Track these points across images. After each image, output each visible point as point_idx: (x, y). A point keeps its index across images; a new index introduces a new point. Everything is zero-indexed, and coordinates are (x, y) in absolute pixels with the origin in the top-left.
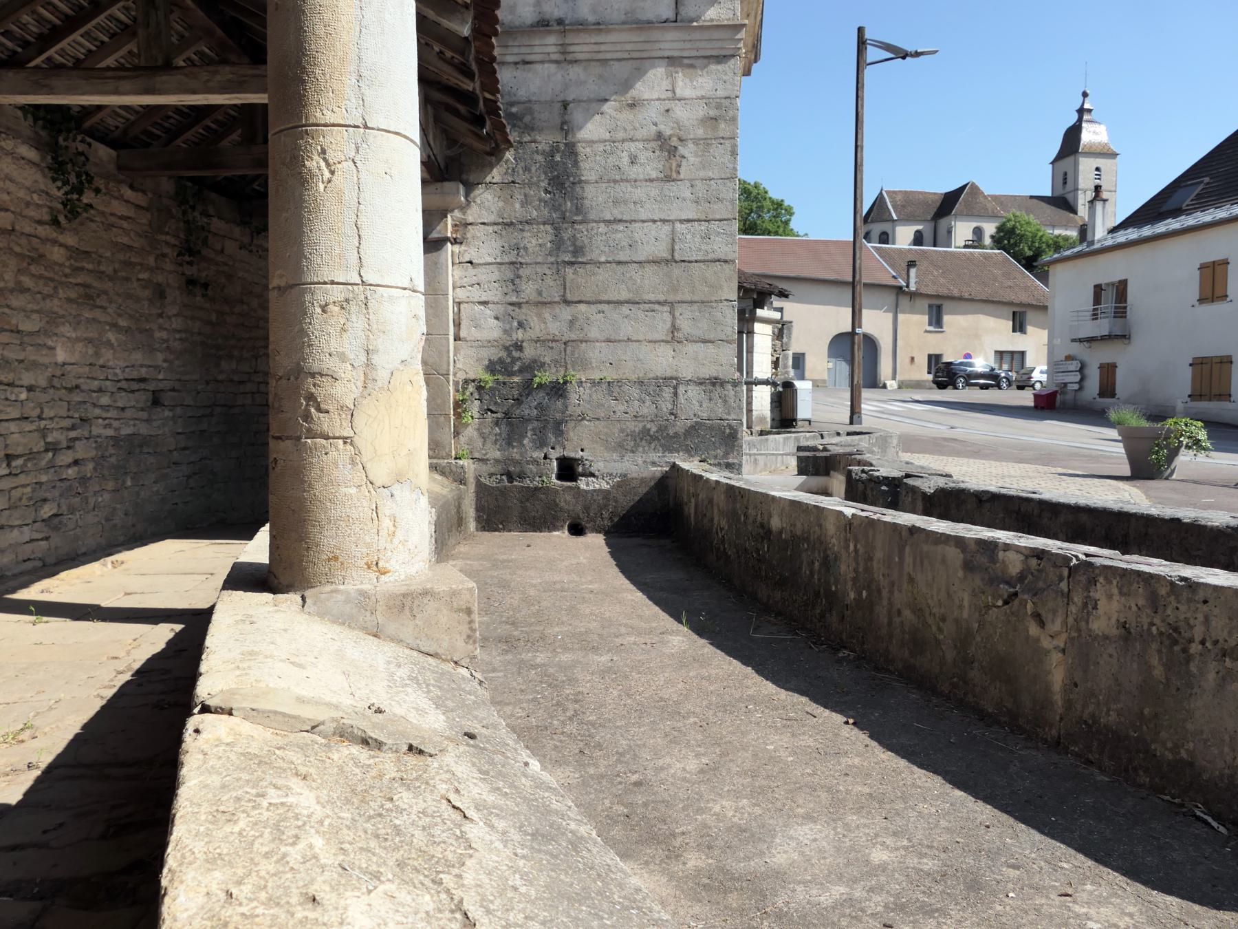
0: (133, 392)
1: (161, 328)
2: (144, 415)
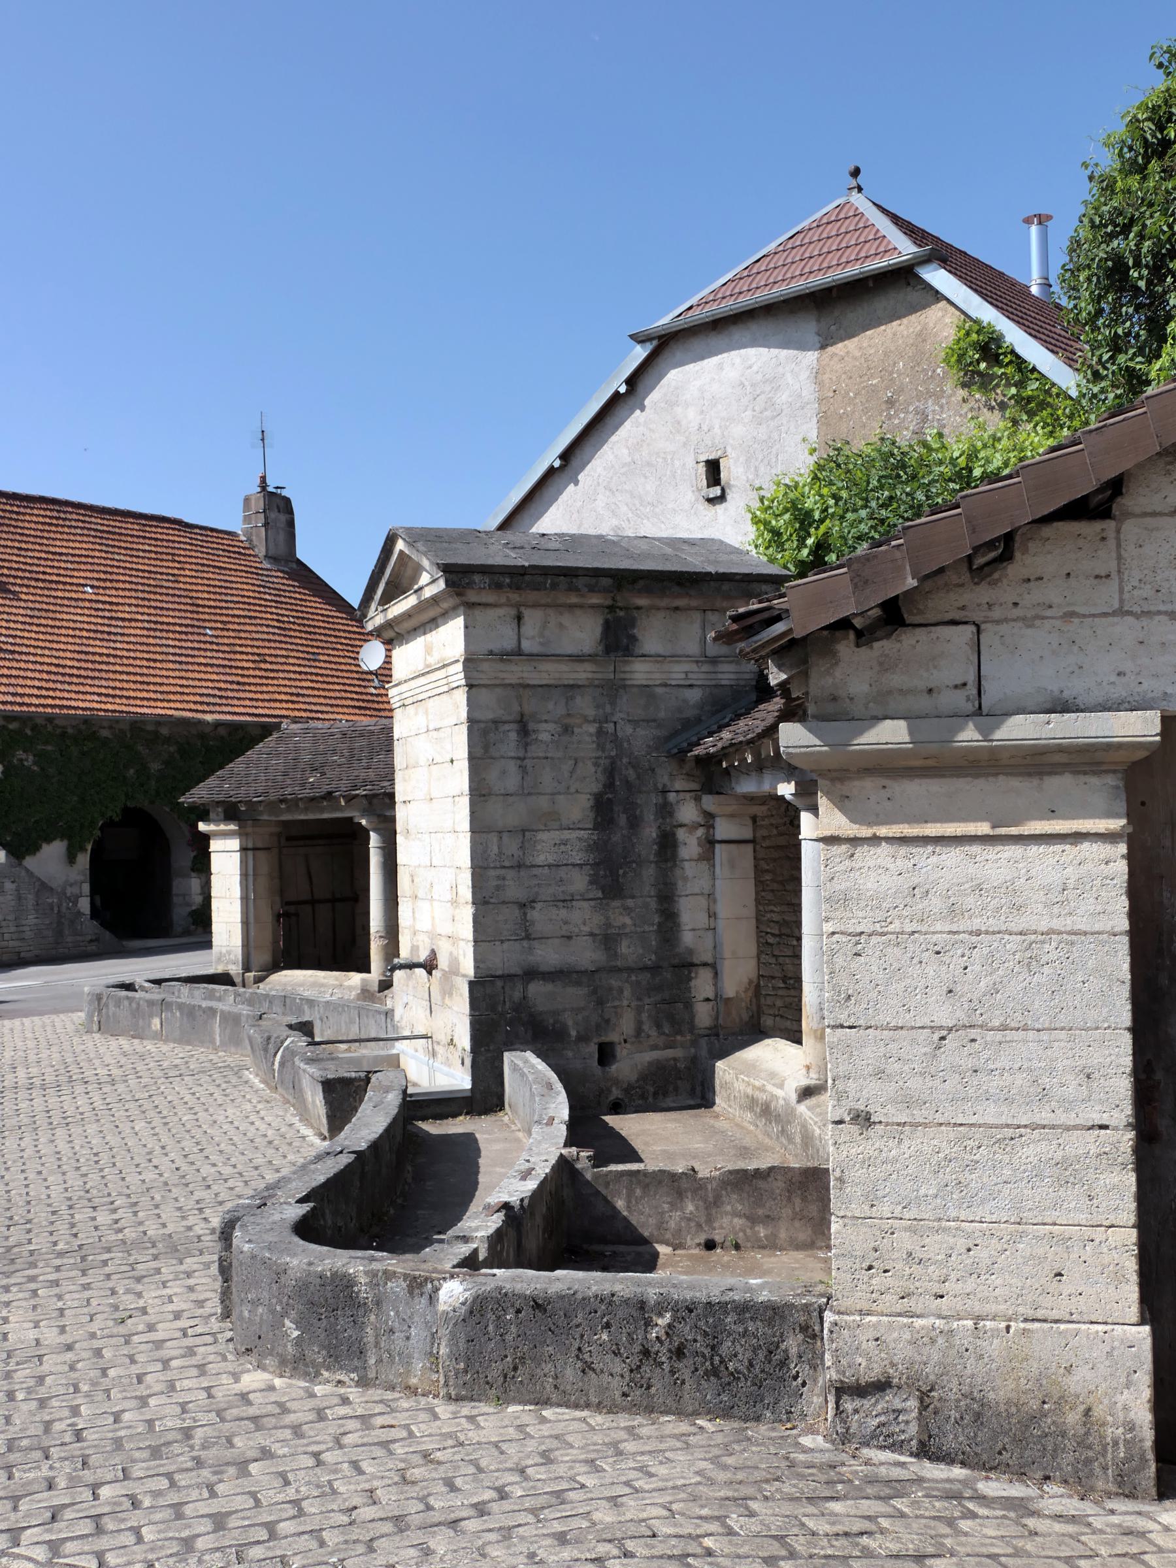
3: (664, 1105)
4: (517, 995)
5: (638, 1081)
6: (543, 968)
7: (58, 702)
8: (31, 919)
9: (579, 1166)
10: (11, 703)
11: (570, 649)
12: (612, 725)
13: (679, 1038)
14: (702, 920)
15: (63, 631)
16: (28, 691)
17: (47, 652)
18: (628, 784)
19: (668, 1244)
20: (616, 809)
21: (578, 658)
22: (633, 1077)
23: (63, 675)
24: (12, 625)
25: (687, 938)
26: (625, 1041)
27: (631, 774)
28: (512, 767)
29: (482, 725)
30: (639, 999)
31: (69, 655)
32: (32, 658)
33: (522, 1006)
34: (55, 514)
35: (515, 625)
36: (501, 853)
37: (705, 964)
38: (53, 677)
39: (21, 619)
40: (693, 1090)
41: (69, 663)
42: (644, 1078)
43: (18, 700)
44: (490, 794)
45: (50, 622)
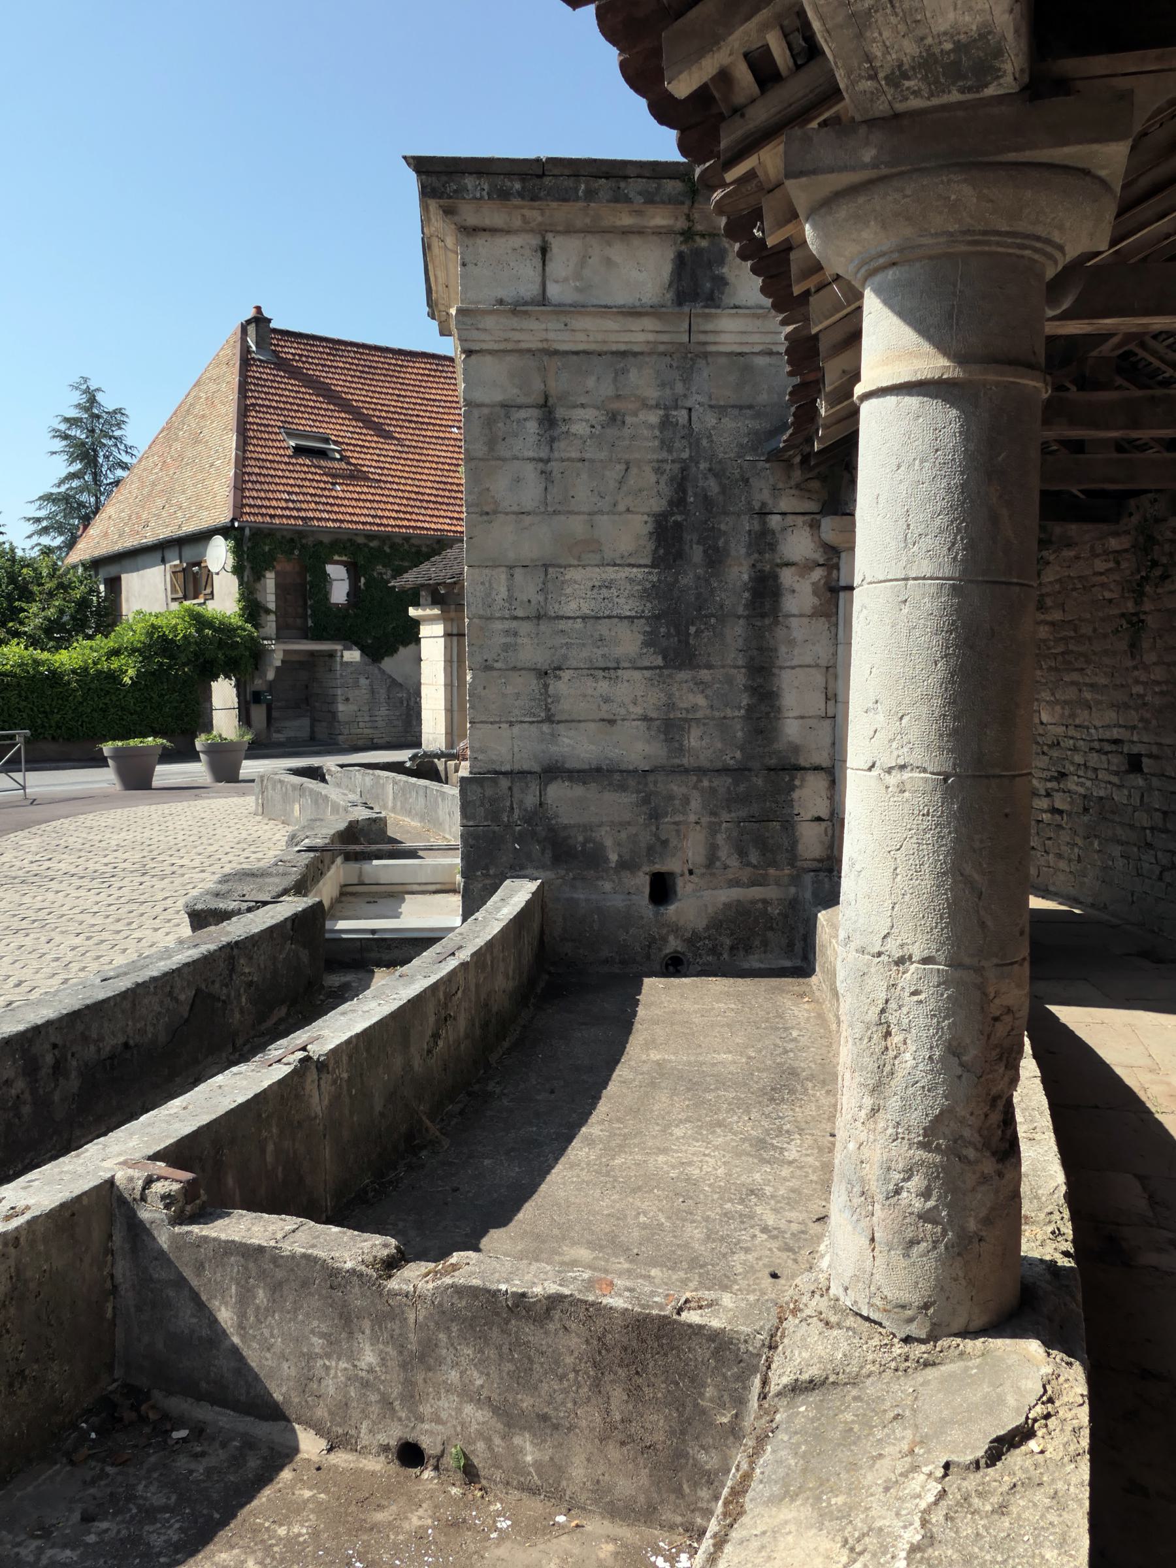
0: (1106, 753)
1: (1137, 682)
2: (1115, 779)
3: (746, 966)
4: (531, 800)
5: (707, 928)
6: (568, 765)
7: (412, 524)
8: (383, 711)
9: (145, 1214)
10: (370, 524)
11: (621, 297)
12: (684, 413)
13: (772, 871)
14: (815, 703)
15: (427, 465)
16: (387, 514)
17: (410, 482)
18: (707, 501)
19: (320, 1432)
20: (687, 537)
21: (633, 312)
22: (701, 924)
23: (421, 501)
24: (382, 459)
25: (791, 729)
26: (691, 872)
27: (713, 486)
28: (530, 472)
29: (486, 411)
30: (713, 813)
31: (429, 484)
32: (395, 486)
33: (538, 814)
34: (434, 367)
35: (537, 261)
36: (511, 598)
37: (817, 768)
38: (412, 503)
39: (391, 454)
40: (791, 945)
41: (428, 491)
42: (717, 924)
43: (378, 521)
44: (495, 512)
45: (417, 457)
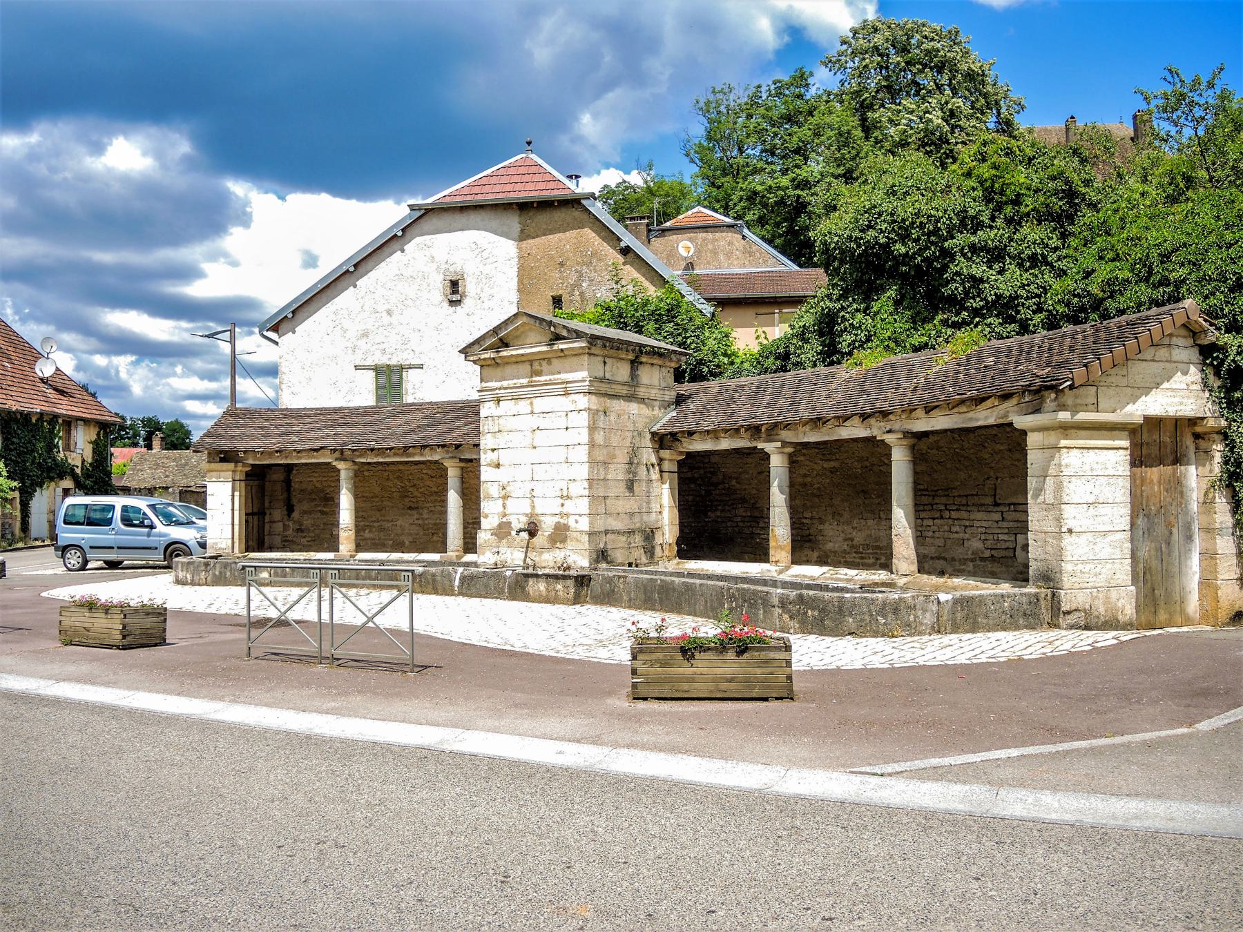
21: (624, 384)
